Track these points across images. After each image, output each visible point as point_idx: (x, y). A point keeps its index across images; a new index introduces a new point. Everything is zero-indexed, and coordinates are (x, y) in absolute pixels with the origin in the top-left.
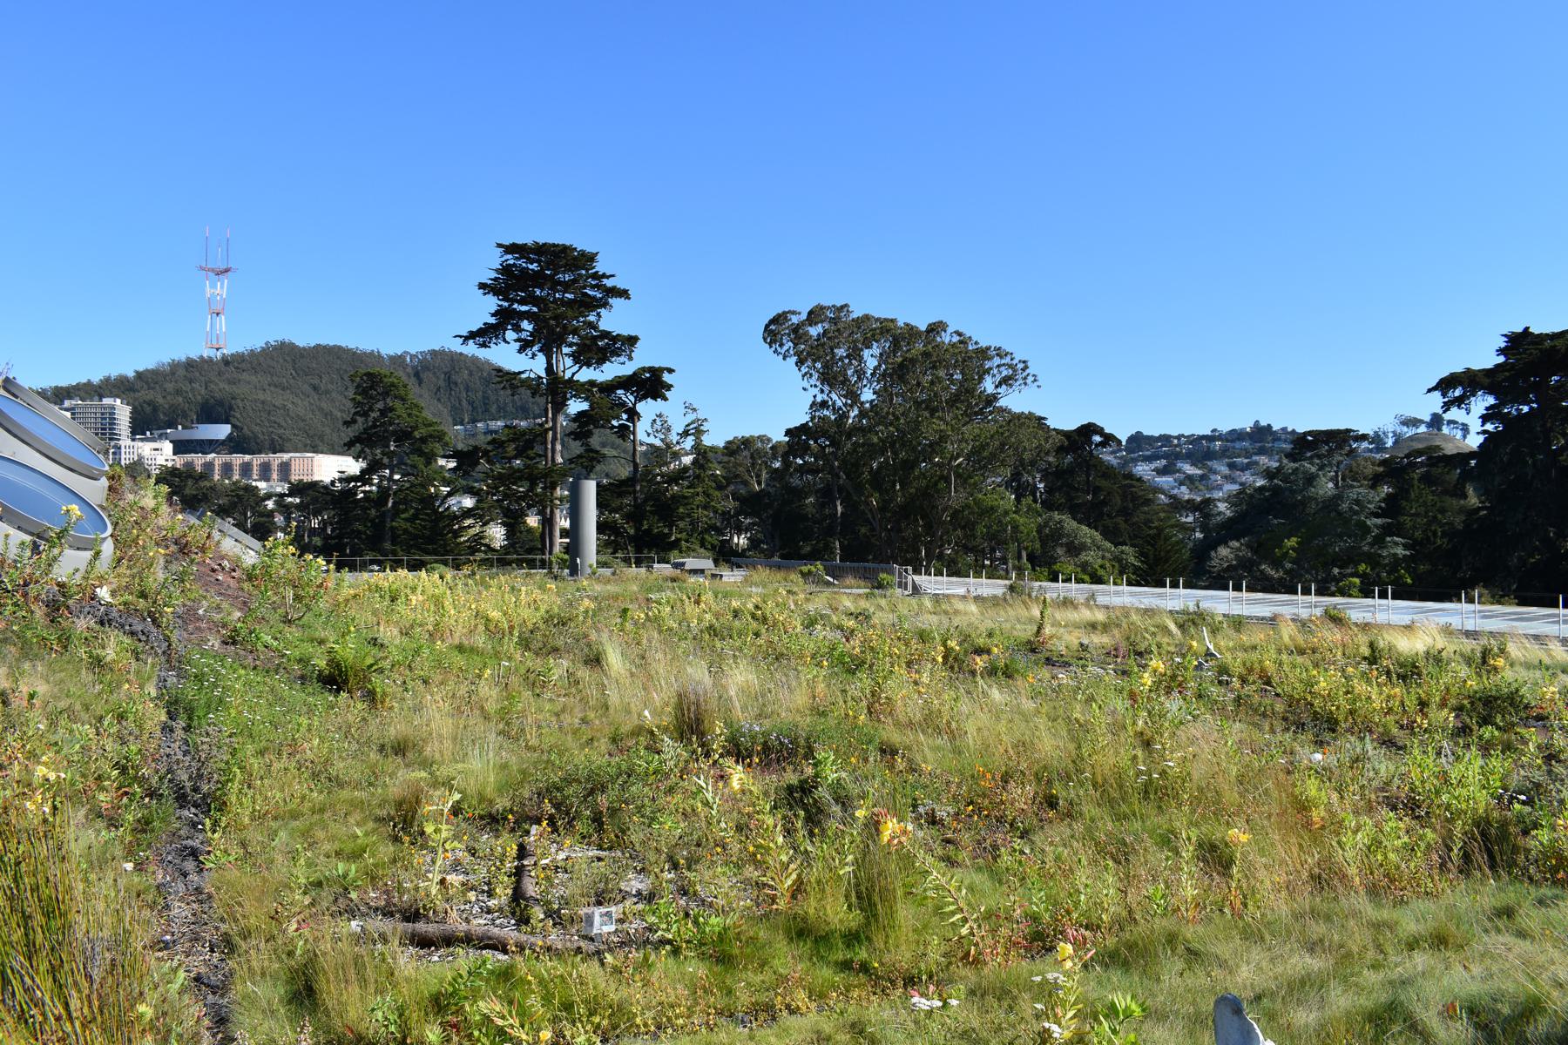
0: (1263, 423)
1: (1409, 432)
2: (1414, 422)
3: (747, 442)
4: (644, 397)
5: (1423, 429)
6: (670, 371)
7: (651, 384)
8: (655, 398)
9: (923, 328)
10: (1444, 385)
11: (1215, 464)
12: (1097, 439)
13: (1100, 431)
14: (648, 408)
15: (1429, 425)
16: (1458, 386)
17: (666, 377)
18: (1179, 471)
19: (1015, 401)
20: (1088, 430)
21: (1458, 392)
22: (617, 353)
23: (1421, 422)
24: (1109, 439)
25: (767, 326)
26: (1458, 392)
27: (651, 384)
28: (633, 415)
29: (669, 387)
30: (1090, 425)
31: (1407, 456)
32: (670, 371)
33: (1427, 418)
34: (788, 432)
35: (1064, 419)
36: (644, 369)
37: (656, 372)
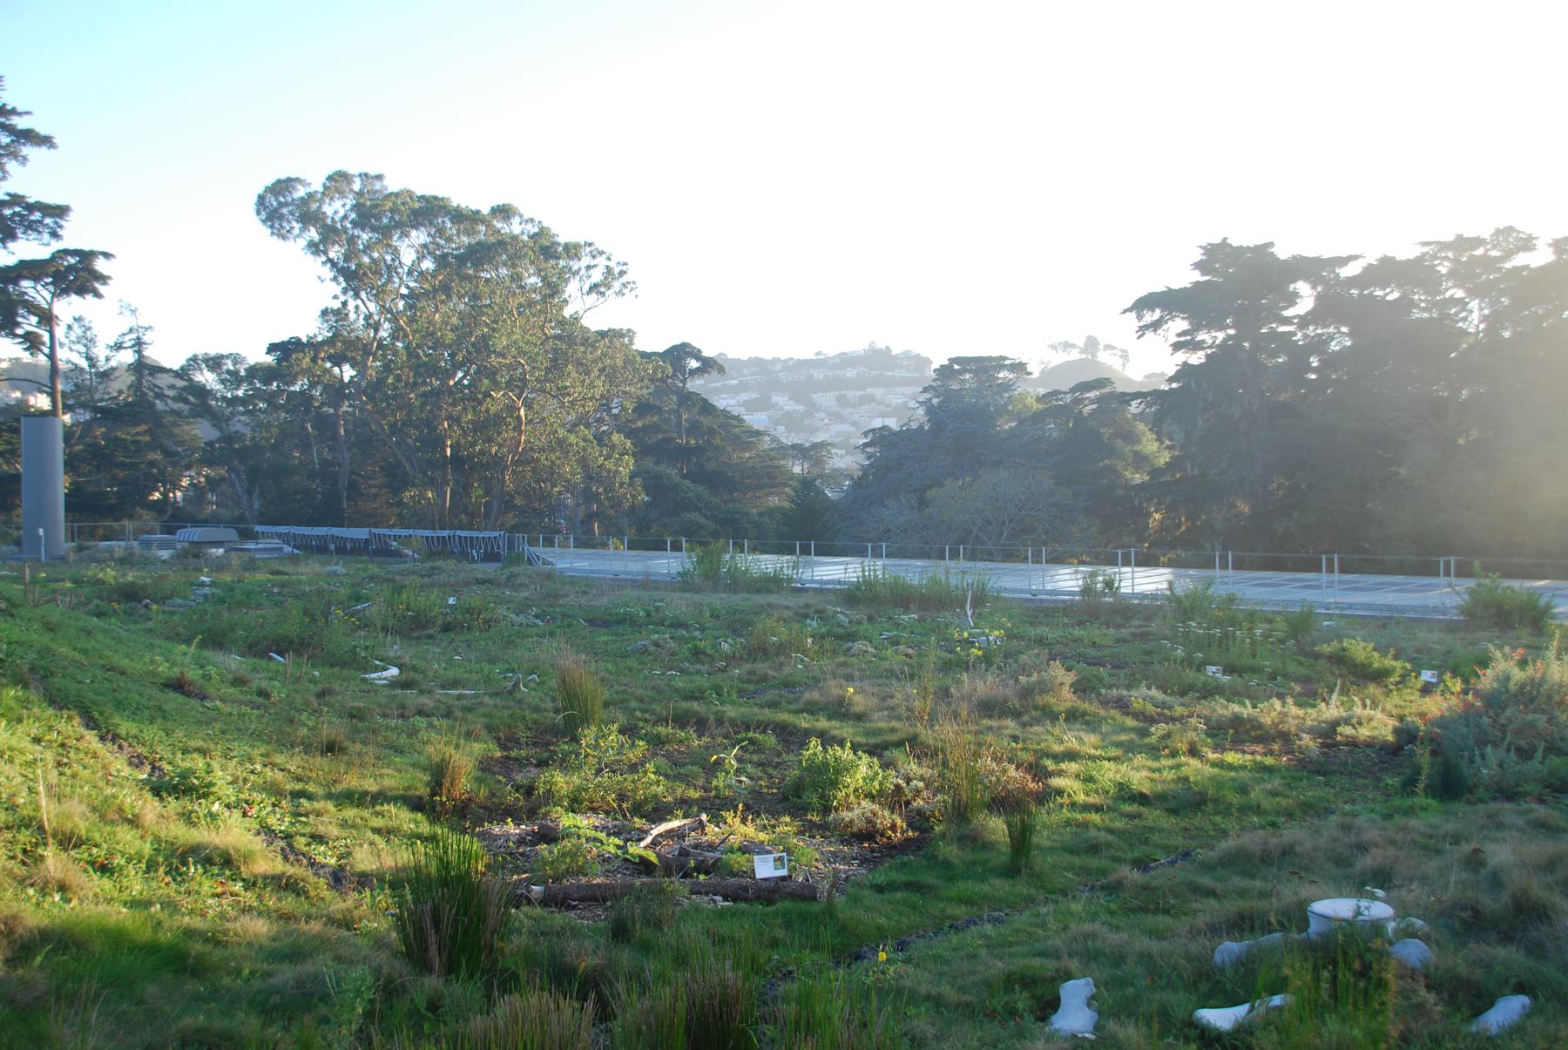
0: (880, 345)
1: (1057, 359)
2: (1067, 346)
3: (214, 363)
4: (65, 292)
5: (1075, 355)
6: (107, 255)
7: (78, 274)
8: (81, 291)
9: (485, 211)
10: (1143, 304)
11: (818, 397)
12: (694, 364)
13: (696, 354)
14: (67, 308)
15: (1083, 351)
16: (1157, 305)
17: (101, 265)
18: (774, 406)
19: (597, 315)
20: (679, 353)
21: (1157, 314)
22: (31, 227)
23: (1073, 346)
24: (708, 365)
25: (261, 199)
26: (1157, 314)
27: (78, 274)
28: (47, 318)
29: (103, 279)
30: (684, 345)
31: (1072, 390)
32: (107, 255)
33: (1081, 343)
34: (272, 348)
35: (652, 339)
36: (67, 252)
37: (86, 257)
